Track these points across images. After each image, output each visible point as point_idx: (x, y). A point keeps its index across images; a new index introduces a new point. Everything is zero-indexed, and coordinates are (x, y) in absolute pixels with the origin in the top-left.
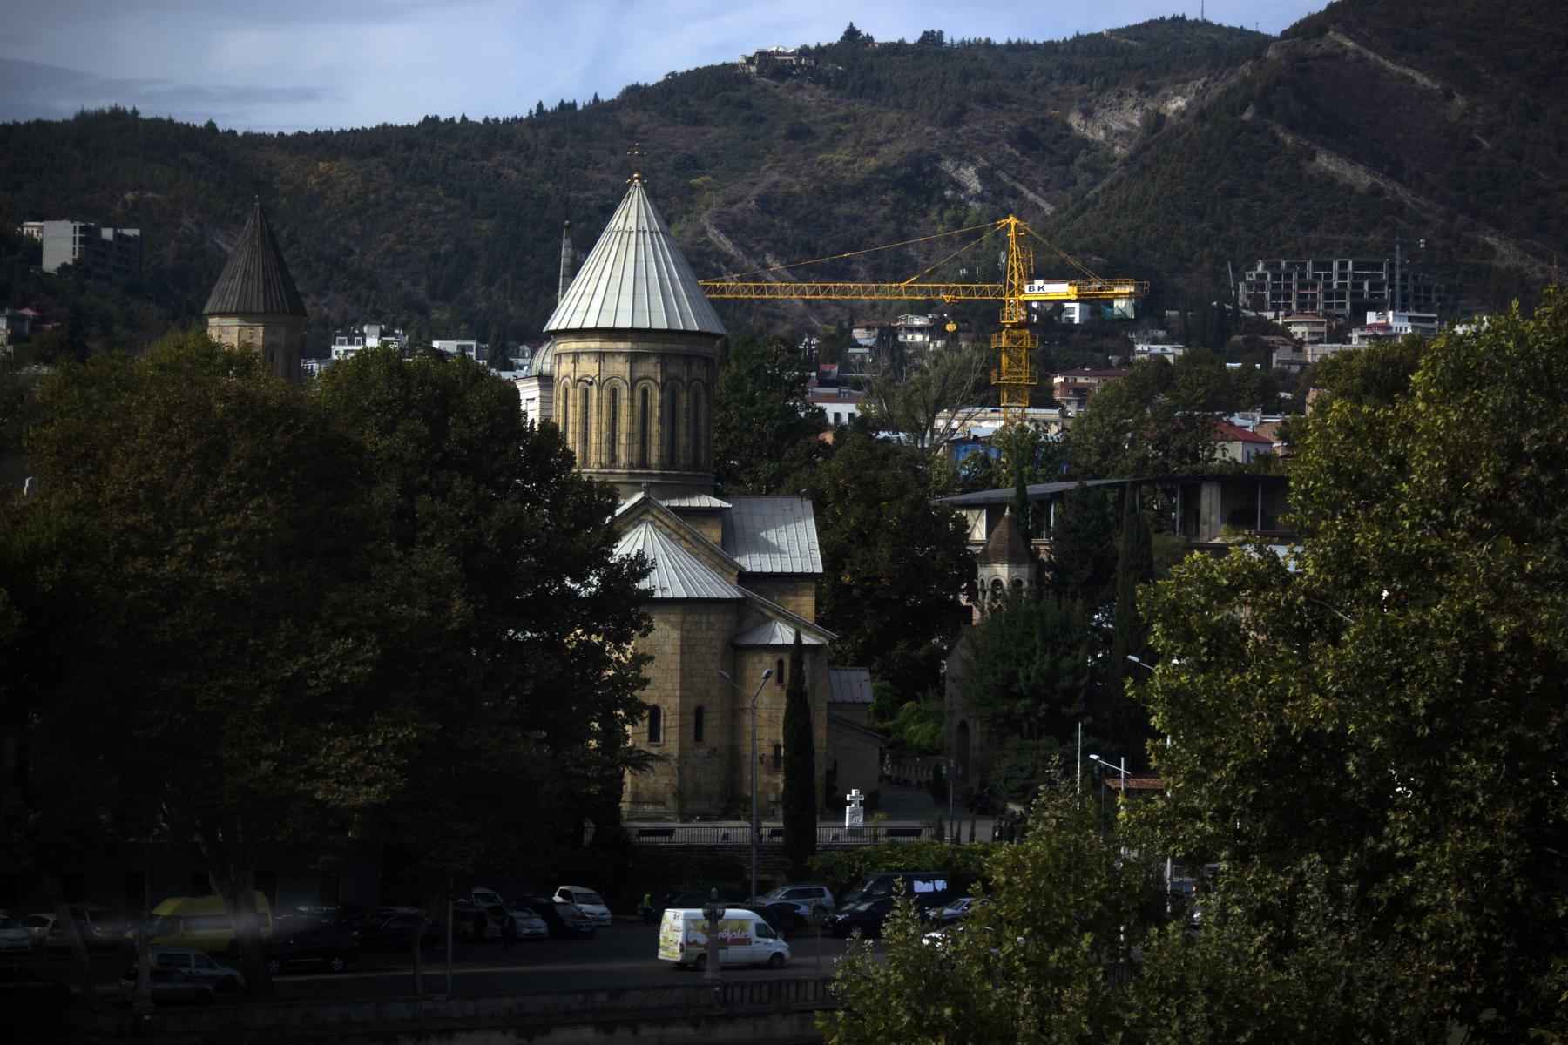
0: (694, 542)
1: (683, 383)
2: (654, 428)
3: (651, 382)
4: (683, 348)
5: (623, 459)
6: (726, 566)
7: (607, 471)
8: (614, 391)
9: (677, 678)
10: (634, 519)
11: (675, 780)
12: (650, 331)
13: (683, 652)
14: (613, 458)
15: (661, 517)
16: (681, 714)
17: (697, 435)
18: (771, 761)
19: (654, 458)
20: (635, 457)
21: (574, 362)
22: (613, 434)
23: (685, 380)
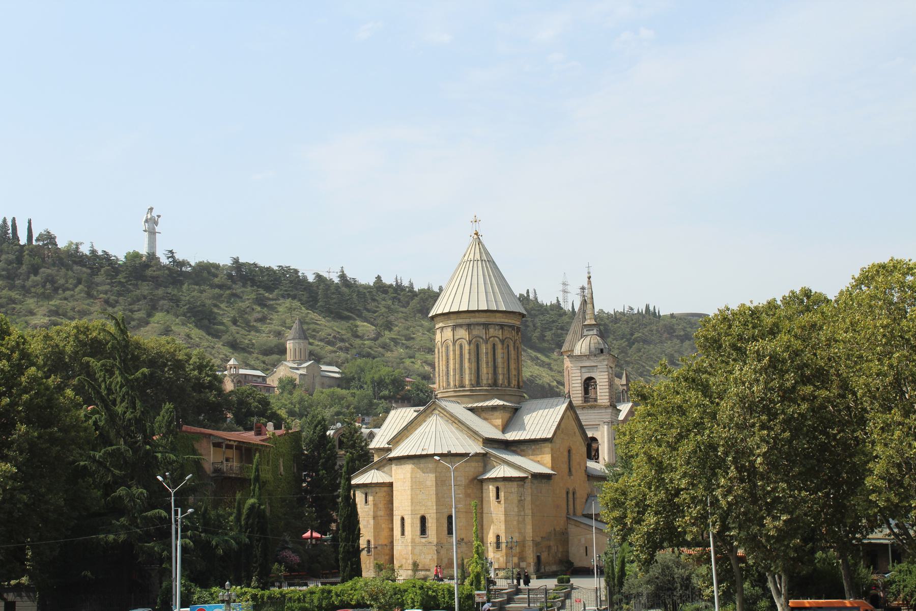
0: (460, 424)
1: (483, 339)
2: (466, 365)
3: (463, 340)
4: (483, 320)
6: (476, 436)
7: (445, 391)
8: (447, 347)
9: (434, 497)
10: (429, 414)
11: (435, 557)
12: (458, 313)
13: (437, 484)
15: (443, 412)
16: (437, 520)
18: (495, 545)
19: (467, 382)
20: (457, 382)
21: (441, 332)
22: (448, 370)
23: (484, 337)
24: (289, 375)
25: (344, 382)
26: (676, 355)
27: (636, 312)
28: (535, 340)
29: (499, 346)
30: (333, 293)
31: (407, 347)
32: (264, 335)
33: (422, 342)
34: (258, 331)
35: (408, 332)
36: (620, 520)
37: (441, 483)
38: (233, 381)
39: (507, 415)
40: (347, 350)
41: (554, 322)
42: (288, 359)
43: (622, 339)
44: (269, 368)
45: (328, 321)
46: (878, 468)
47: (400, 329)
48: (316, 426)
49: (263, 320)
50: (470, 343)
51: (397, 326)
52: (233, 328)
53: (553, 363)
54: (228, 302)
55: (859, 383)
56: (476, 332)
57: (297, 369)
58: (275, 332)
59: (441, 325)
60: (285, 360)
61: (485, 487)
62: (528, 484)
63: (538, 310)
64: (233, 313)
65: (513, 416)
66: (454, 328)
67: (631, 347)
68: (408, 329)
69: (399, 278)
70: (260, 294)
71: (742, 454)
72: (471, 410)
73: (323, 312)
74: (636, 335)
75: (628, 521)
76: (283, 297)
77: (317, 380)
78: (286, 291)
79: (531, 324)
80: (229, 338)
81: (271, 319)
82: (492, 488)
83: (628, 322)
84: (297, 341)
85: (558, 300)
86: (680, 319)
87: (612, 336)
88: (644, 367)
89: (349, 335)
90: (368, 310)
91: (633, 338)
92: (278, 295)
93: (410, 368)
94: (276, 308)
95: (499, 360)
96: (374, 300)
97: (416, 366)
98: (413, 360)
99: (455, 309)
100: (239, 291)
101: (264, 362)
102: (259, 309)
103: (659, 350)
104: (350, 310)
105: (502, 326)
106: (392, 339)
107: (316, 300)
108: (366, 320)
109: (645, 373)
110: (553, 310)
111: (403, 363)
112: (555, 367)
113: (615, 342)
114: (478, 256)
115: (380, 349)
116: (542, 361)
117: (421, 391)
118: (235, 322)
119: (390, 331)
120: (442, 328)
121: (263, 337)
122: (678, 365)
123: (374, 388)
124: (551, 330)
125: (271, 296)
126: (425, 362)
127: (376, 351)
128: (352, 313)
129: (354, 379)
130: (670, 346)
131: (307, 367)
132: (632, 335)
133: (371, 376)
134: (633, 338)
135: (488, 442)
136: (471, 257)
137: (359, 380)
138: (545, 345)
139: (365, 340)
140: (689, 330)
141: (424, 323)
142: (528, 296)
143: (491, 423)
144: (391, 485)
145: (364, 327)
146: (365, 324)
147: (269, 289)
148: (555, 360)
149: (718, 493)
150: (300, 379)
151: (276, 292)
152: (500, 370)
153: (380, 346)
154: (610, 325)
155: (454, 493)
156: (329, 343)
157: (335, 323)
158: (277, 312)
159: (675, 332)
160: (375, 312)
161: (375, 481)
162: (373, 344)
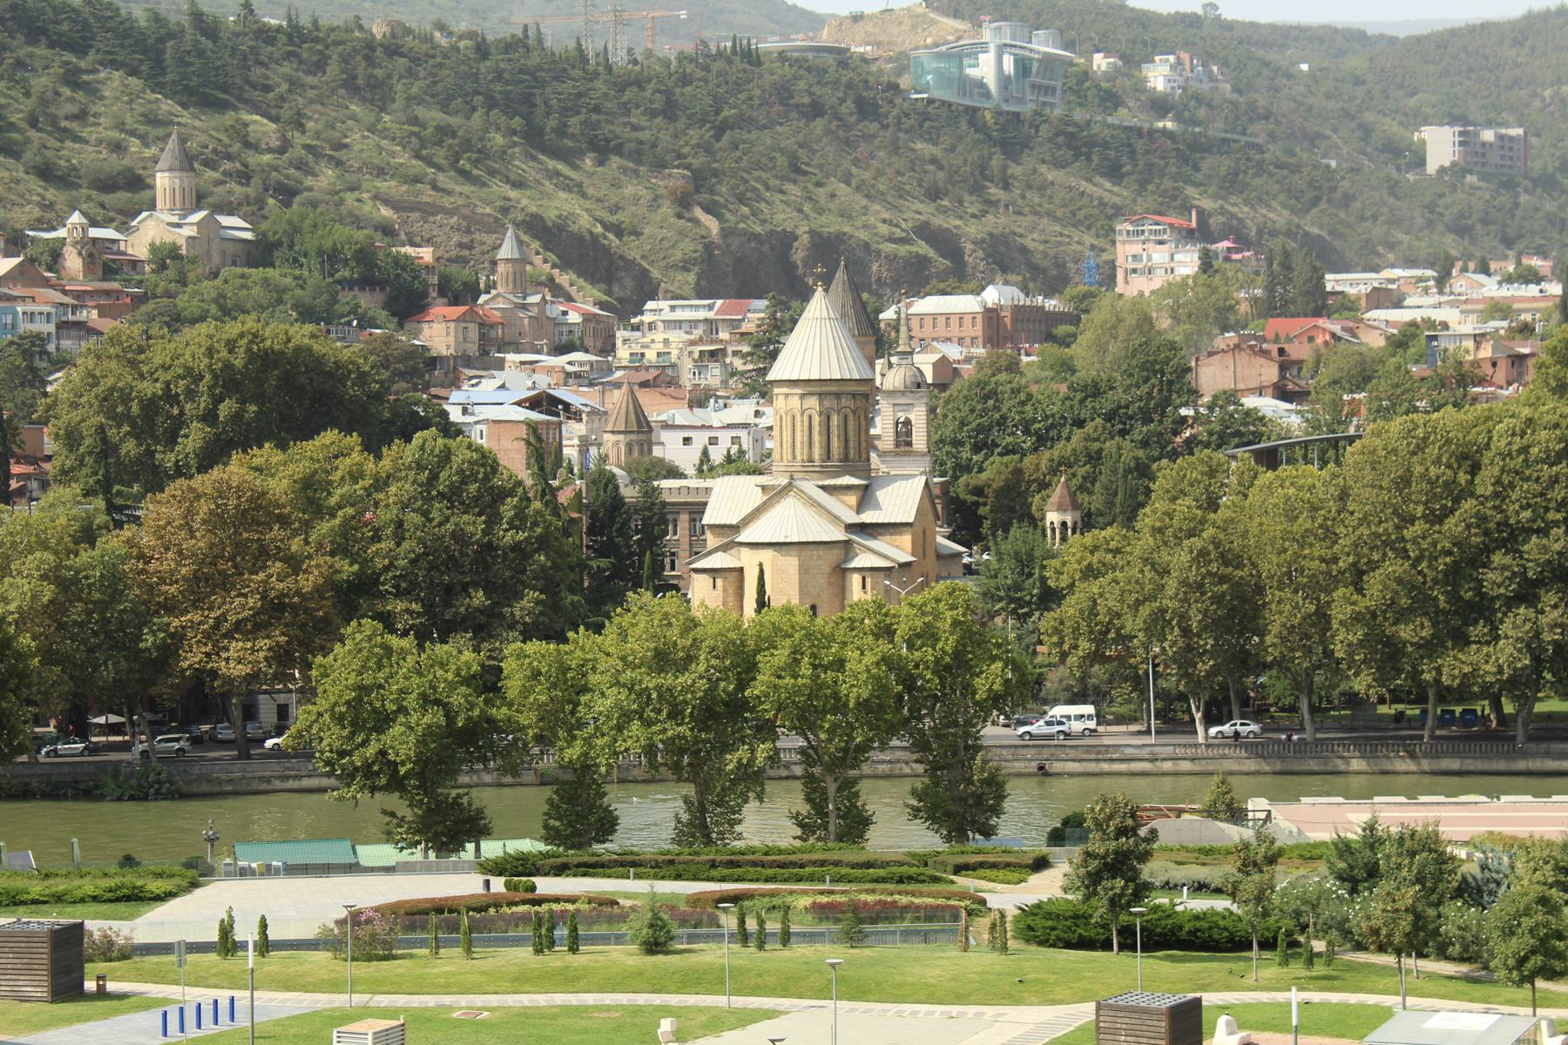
2: (816, 437)
4: (834, 389)
5: (799, 457)
14: (794, 457)
17: (846, 441)
19: (816, 457)
24: (168, 239)
25: (260, 253)
26: (802, 153)
27: (714, 51)
28: (549, 136)
29: (851, 417)
30: (189, 53)
31: (339, 163)
32: (91, 149)
33: (364, 155)
34: (78, 139)
35: (336, 134)
36: (1060, 644)
37: (803, 570)
38: (80, 254)
39: (860, 493)
40: (244, 177)
41: (580, 95)
42: (159, 205)
43: (703, 122)
44: (125, 217)
45: (196, 117)
46: (1275, 629)
47: (319, 126)
48: (606, 485)
49: (81, 116)
50: (820, 414)
51: (310, 118)
52: (32, 133)
53: (587, 182)
54: (10, 80)
55: (1265, 568)
56: (826, 403)
57: (179, 226)
58: (109, 144)
59: (785, 390)
60: (152, 206)
61: (848, 575)
62: (895, 574)
63: (550, 71)
64: (28, 105)
65: (865, 497)
66: (802, 396)
67: (718, 138)
68: (333, 128)
69: (293, 12)
70: (67, 63)
71: (1183, 617)
72: (822, 487)
73: (176, 93)
74: (725, 113)
75: (1066, 647)
76: (101, 64)
77: (215, 246)
78: (108, 53)
79: (538, 101)
80: (38, 158)
81: (94, 116)
82: (856, 579)
83: (706, 81)
84: (177, 174)
85: (579, 43)
86: (797, 61)
87: (684, 120)
88: (746, 181)
89: (236, 148)
90: (253, 85)
91: (720, 118)
92: (95, 62)
93: (357, 212)
94: (98, 90)
95: (851, 433)
96: (261, 64)
97: (367, 207)
98: (356, 194)
99: (804, 377)
100: (21, 53)
101: (102, 206)
102: (66, 92)
103: (769, 142)
104: (225, 89)
105: (854, 396)
106: (307, 147)
107: (158, 66)
108: (257, 108)
109: (749, 195)
110: (574, 67)
111: (342, 202)
112: (590, 191)
113: (691, 132)
114: (825, 314)
115: (292, 171)
116: (567, 178)
117: (404, 269)
118: (33, 122)
119: (303, 132)
120: (787, 395)
121: (86, 156)
122: (806, 173)
123: (322, 263)
124: (578, 113)
125: (83, 65)
126: (375, 197)
127: (288, 177)
128: (226, 92)
129: (279, 244)
130: (787, 134)
131: (198, 224)
132: (718, 112)
133: (316, 243)
134: (720, 118)
135: (851, 528)
136: (818, 314)
137: (291, 246)
138: (570, 143)
139: (262, 152)
140: (816, 89)
141: (353, 107)
142: (527, 36)
143: (843, 502)
144: (741, 569)
145: (261, 126)
146: (257, 118)
147: (80, 49)
148: (590, 175)
149: (1166, 644)
150: (188, 244)
151: (91, 56)
152: (851, 444)
153: (291, 164)
154: (677, 90)
155: (822, 580)
156: (210, 164)
157: (212, 123)
158: (102, 98)
159: (792, 97)
160: (267, 89)
161: (725, 566)
162: (279, 162)
